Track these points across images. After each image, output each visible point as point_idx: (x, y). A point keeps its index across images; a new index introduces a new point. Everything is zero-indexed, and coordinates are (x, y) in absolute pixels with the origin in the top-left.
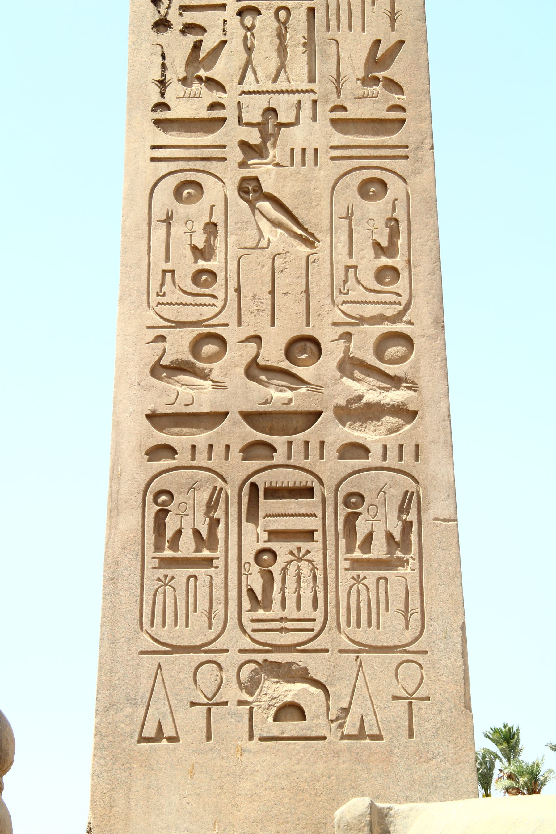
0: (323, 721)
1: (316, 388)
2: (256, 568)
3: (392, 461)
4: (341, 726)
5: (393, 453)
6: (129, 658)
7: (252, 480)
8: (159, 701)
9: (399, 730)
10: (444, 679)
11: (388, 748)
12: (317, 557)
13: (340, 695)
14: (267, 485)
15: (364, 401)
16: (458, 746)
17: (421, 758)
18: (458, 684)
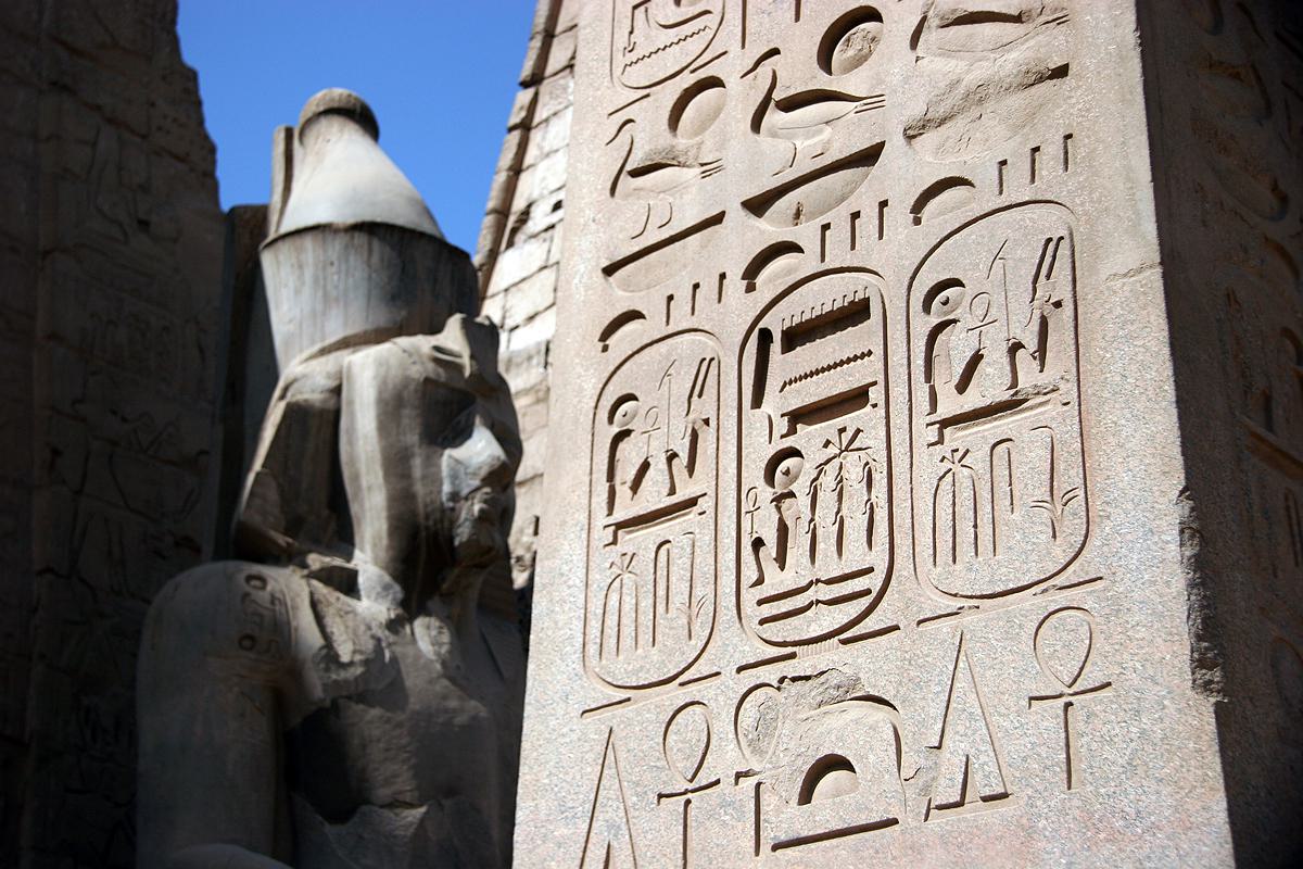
0: (890, 781)
1: (873, 102)
2: (766, 494)
3: (1018, 189)
4: (926, 789)
5: (1017, 174)
6: (565, 730)
7: (761, 325)
8: (610, 803)
9: (1047, 773)
10: (1142, 633)
11: (1024, 821)
12: (873, 439)
13: (920, 716)
14: (787, 324)
15: (961, 90)
16: (1181, 788)
17: (1098, 831)
18: (1176, 638)
